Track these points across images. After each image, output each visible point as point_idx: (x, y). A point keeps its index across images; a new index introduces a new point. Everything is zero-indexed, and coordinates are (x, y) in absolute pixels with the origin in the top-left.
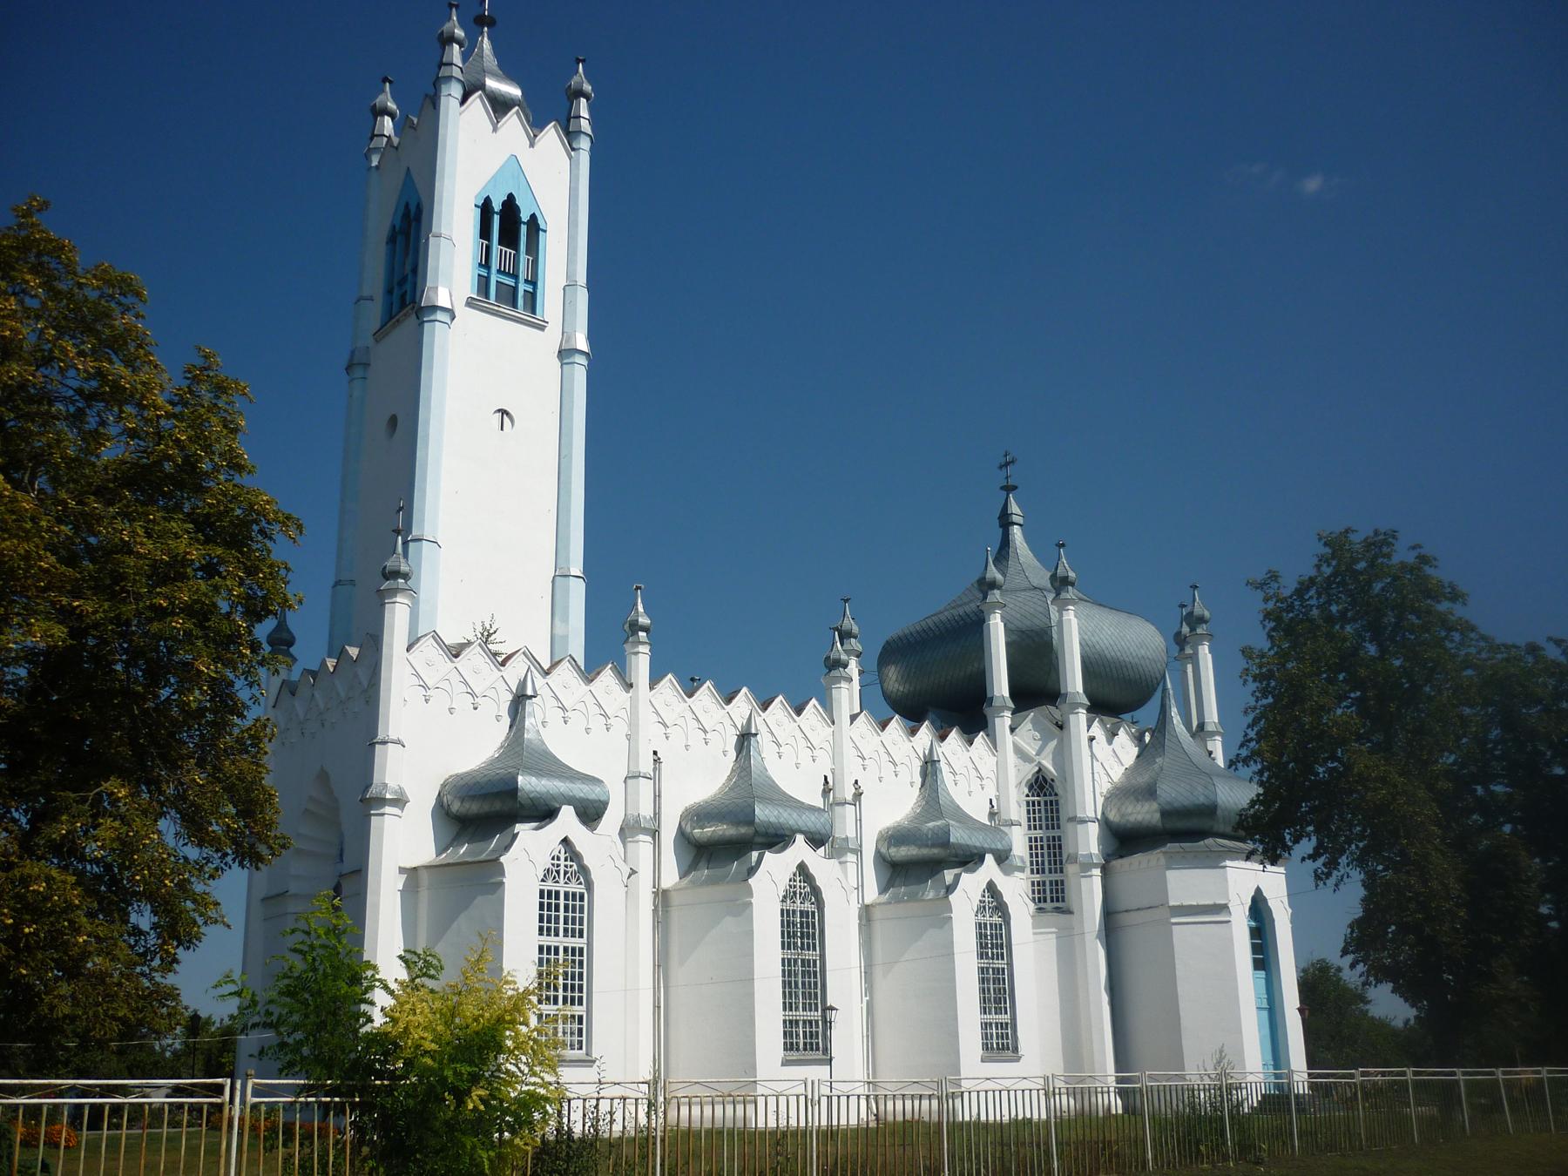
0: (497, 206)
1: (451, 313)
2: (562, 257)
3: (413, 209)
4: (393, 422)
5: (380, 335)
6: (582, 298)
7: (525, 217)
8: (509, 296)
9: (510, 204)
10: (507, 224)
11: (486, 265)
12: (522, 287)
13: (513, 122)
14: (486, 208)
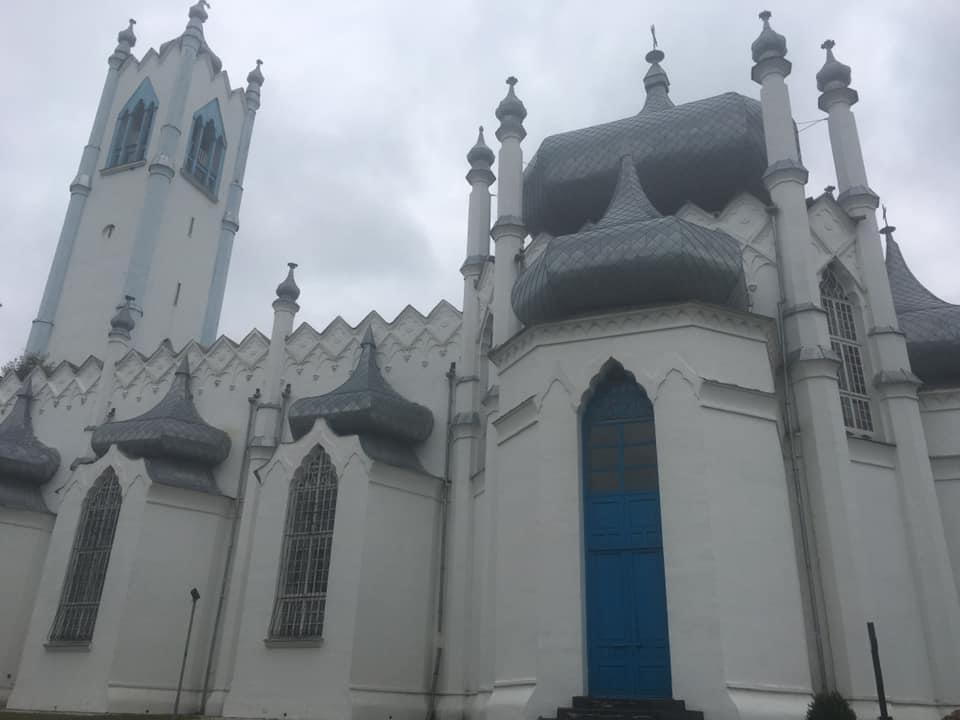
0: (204, 124)
1: (173, 173)
3: (147, 104)
5: (104, 173)
9: (211, 123)
14: (198, 120)
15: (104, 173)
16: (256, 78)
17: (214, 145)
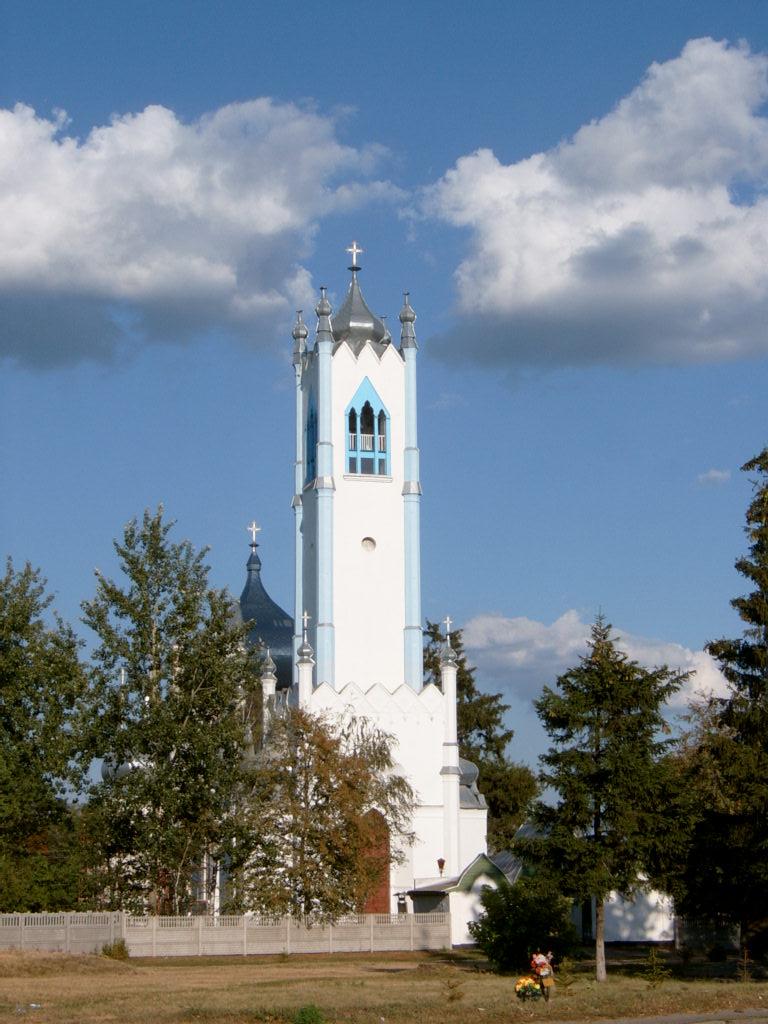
0: (359, 412)
2: (401, 432)
4: (312, 545)
6: (415, 455)
7: (376, 413)
8: (368, 467)
9: (367, 410)
10: (367, 420)
11: (354, 449)
13: (368, 349)
14: (352, 415)
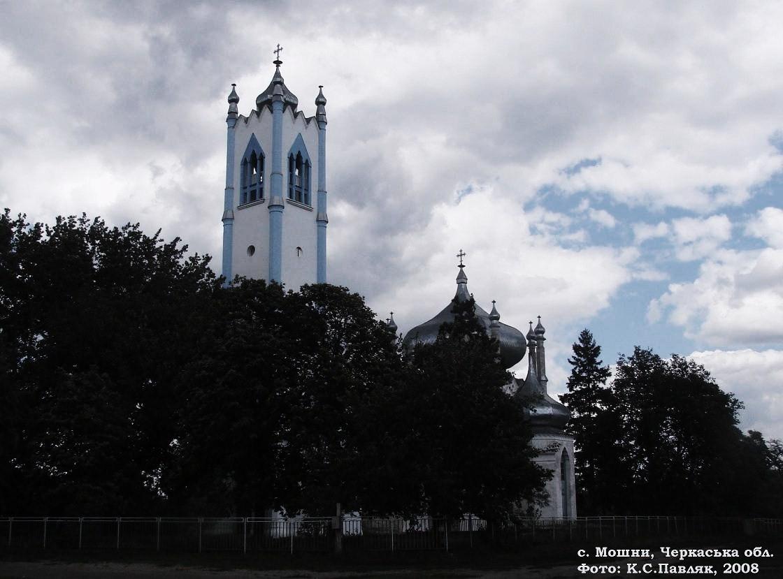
0: (295, 157)
5: (239, 208)
9: (299, 156)
12: (303, 193)
14: (291, 158)
15: (239, 208)
16: (320, 102)
17: (304, 166)
